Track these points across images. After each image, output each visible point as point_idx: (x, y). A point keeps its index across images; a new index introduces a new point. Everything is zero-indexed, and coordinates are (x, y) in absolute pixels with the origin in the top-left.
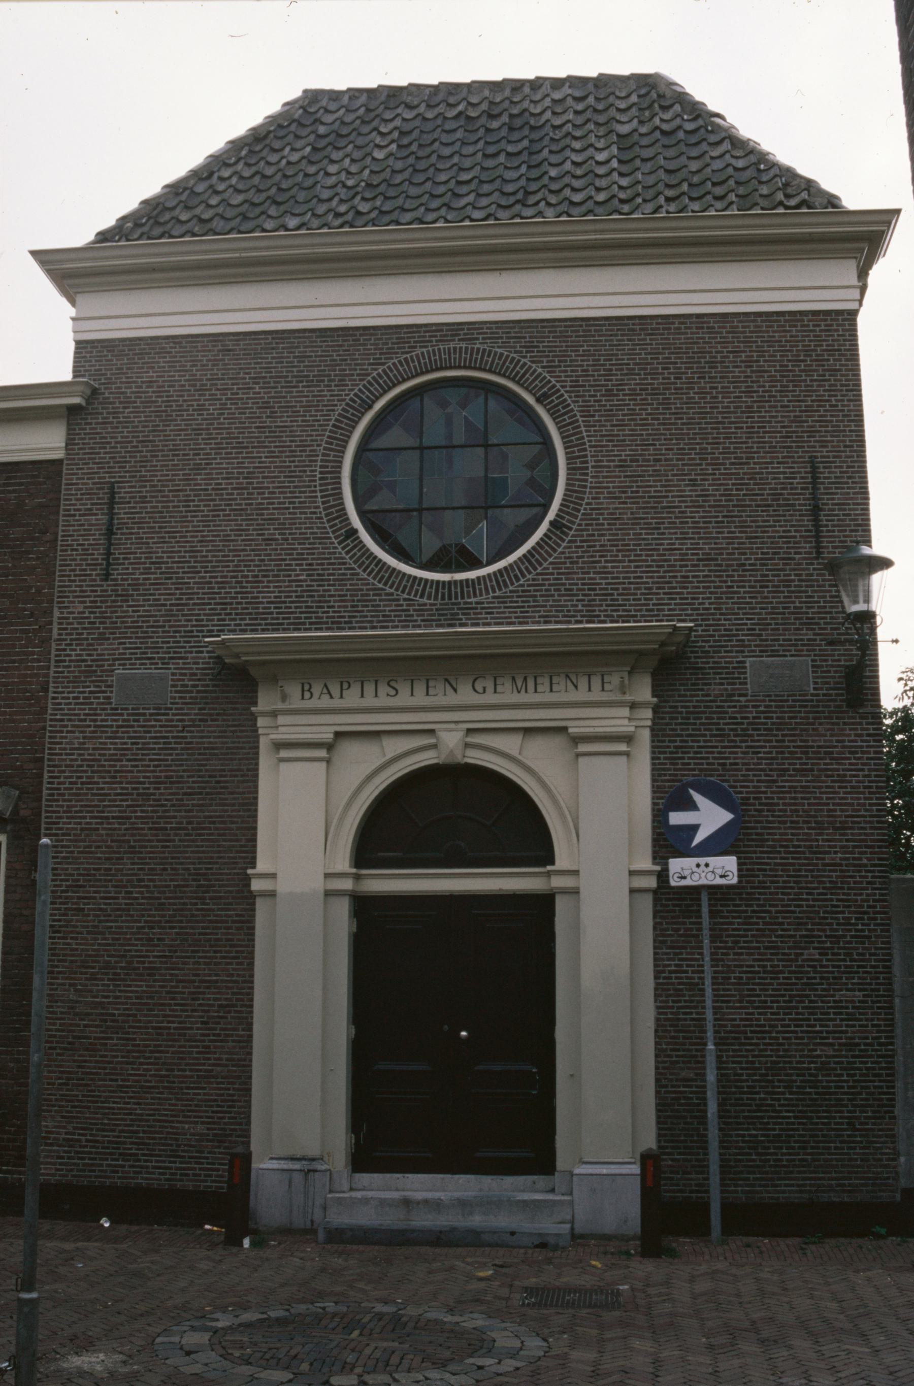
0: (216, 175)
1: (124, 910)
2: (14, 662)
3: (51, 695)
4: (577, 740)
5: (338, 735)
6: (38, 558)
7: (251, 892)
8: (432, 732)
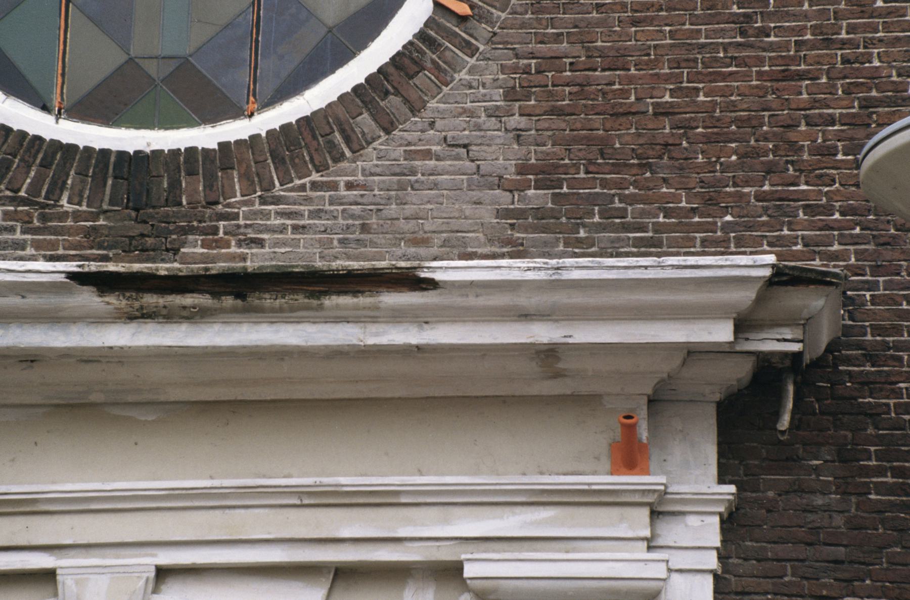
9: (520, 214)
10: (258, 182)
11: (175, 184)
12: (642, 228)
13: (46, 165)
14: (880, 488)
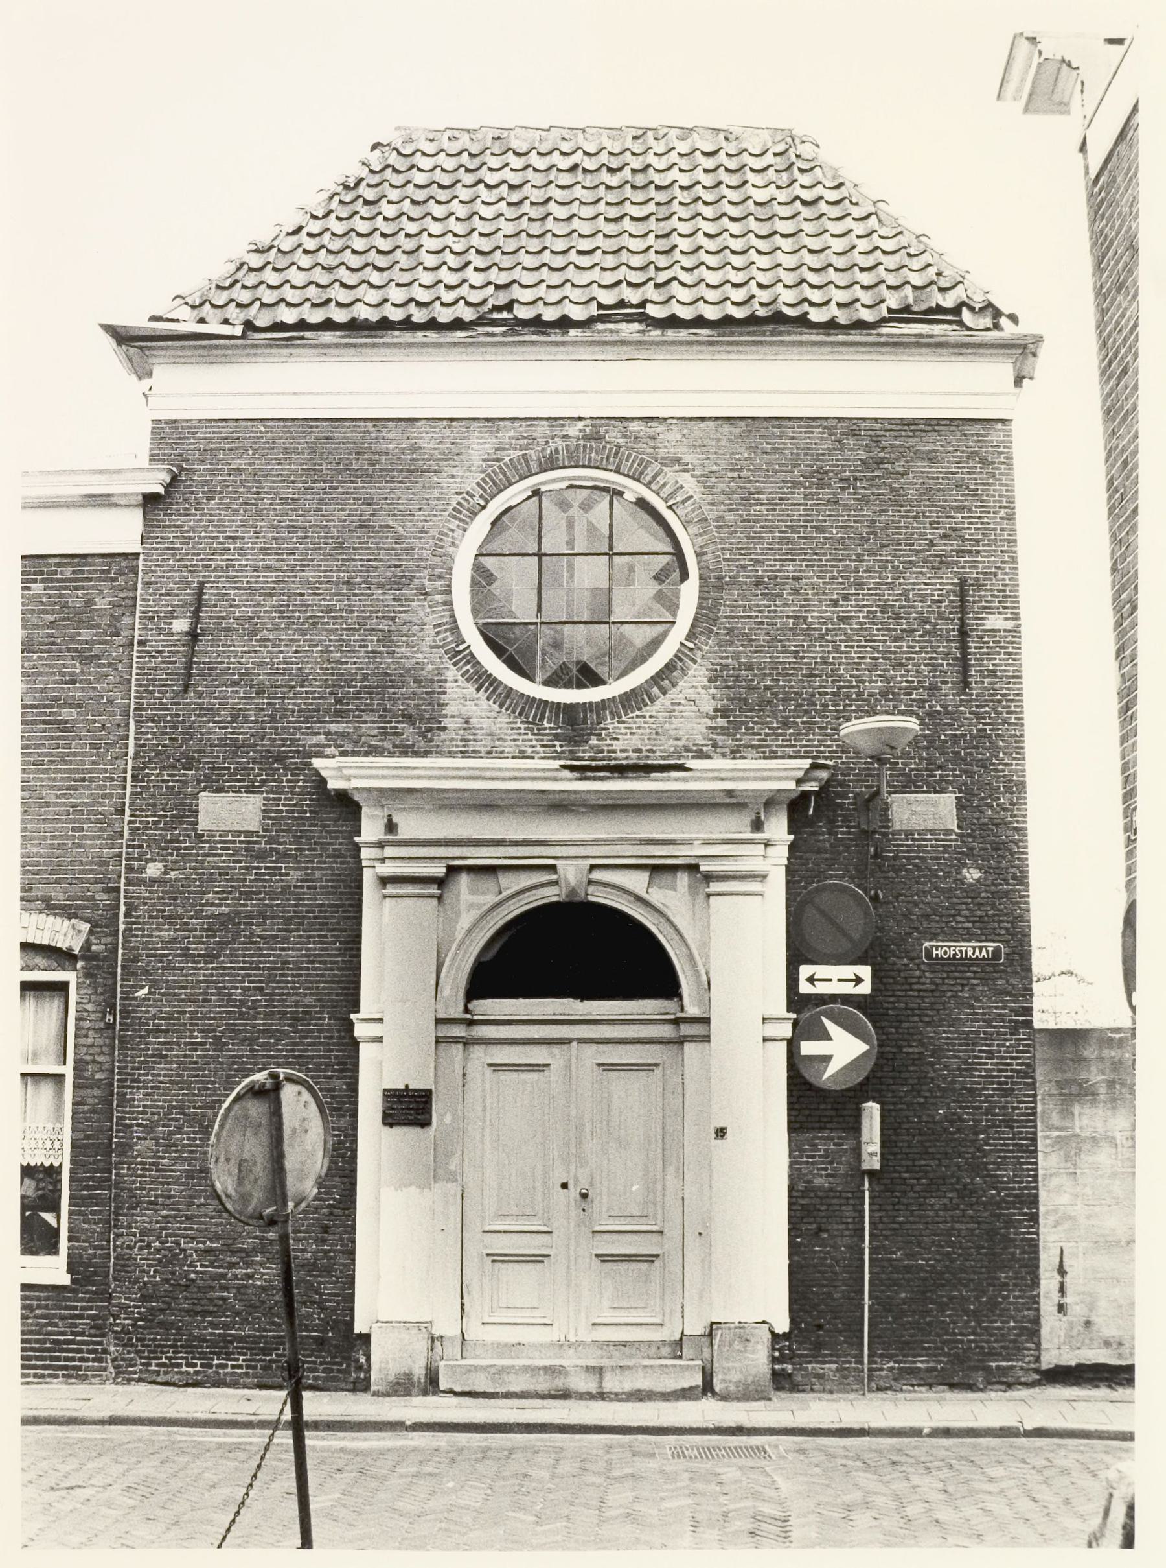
0: (304, 231)
1: (212, 1056)
2: (84, 780)
3: (127, 818)
4: (709, 878)
5: (452, 870)
6: (110, 665)
7: (354, 1039)
8: (553, 868)
9: (715, 728)
10: (615, 715)
11: (585, 717)
12: (760, 734)
13: (538, 708)
14: (843, 833)
